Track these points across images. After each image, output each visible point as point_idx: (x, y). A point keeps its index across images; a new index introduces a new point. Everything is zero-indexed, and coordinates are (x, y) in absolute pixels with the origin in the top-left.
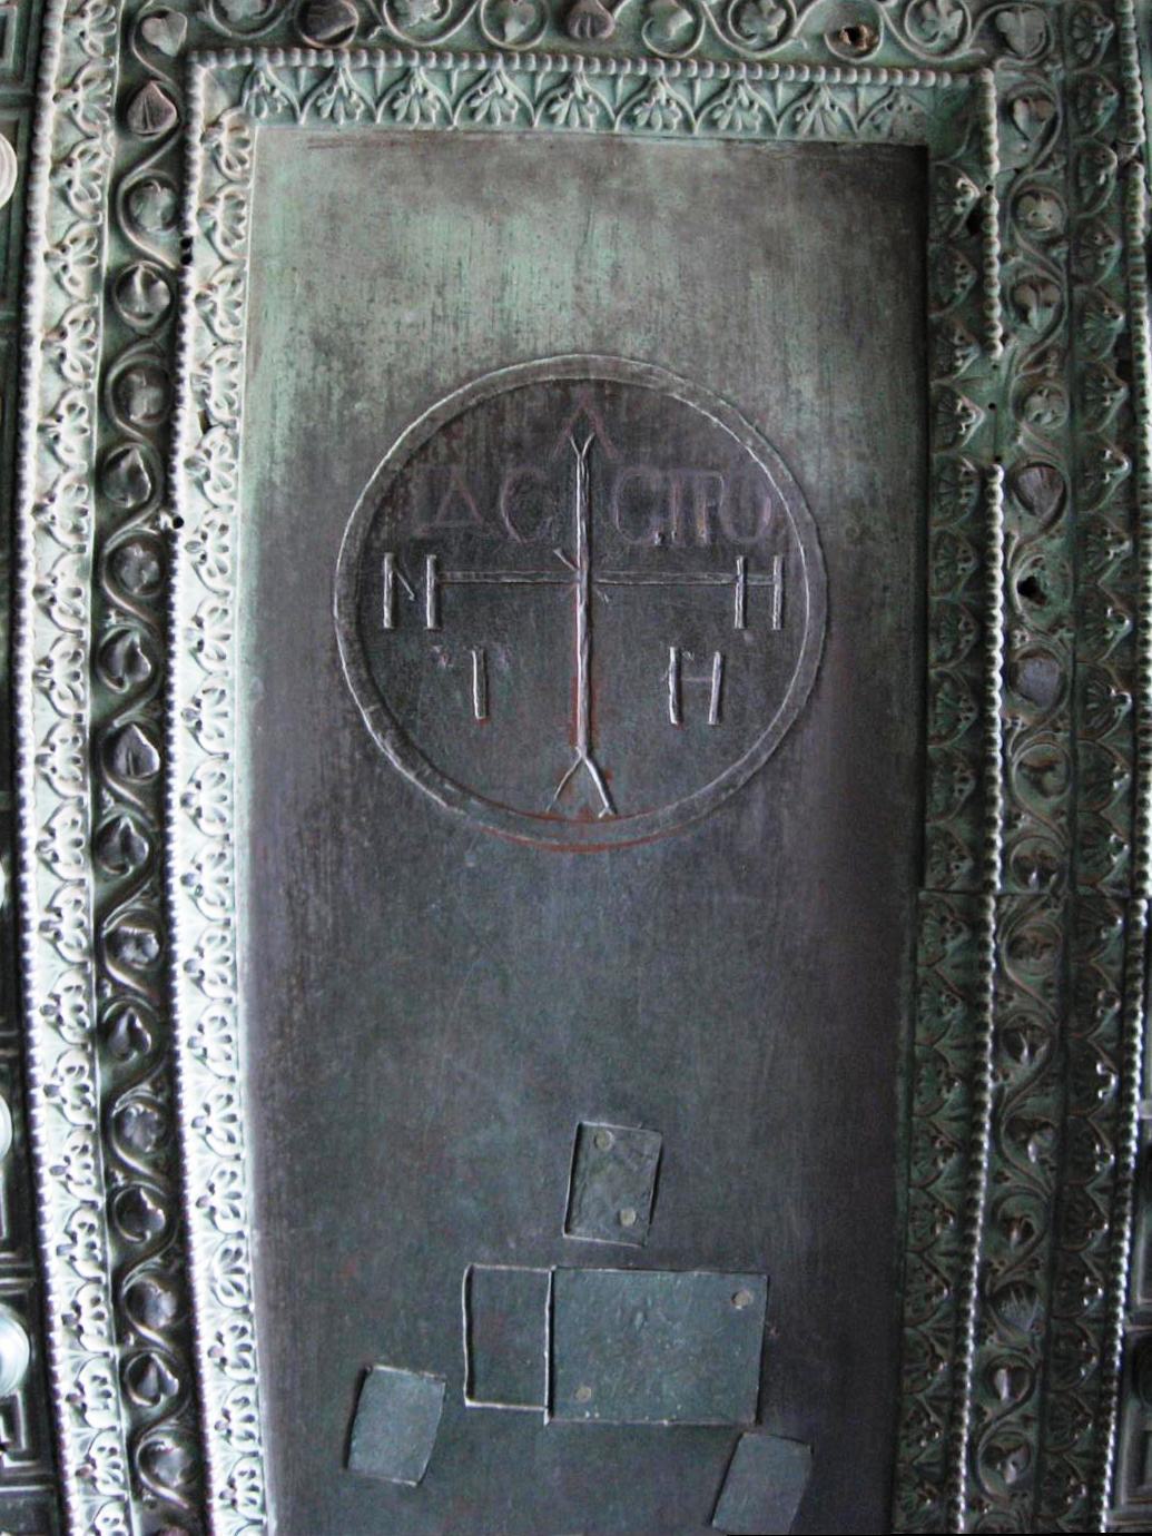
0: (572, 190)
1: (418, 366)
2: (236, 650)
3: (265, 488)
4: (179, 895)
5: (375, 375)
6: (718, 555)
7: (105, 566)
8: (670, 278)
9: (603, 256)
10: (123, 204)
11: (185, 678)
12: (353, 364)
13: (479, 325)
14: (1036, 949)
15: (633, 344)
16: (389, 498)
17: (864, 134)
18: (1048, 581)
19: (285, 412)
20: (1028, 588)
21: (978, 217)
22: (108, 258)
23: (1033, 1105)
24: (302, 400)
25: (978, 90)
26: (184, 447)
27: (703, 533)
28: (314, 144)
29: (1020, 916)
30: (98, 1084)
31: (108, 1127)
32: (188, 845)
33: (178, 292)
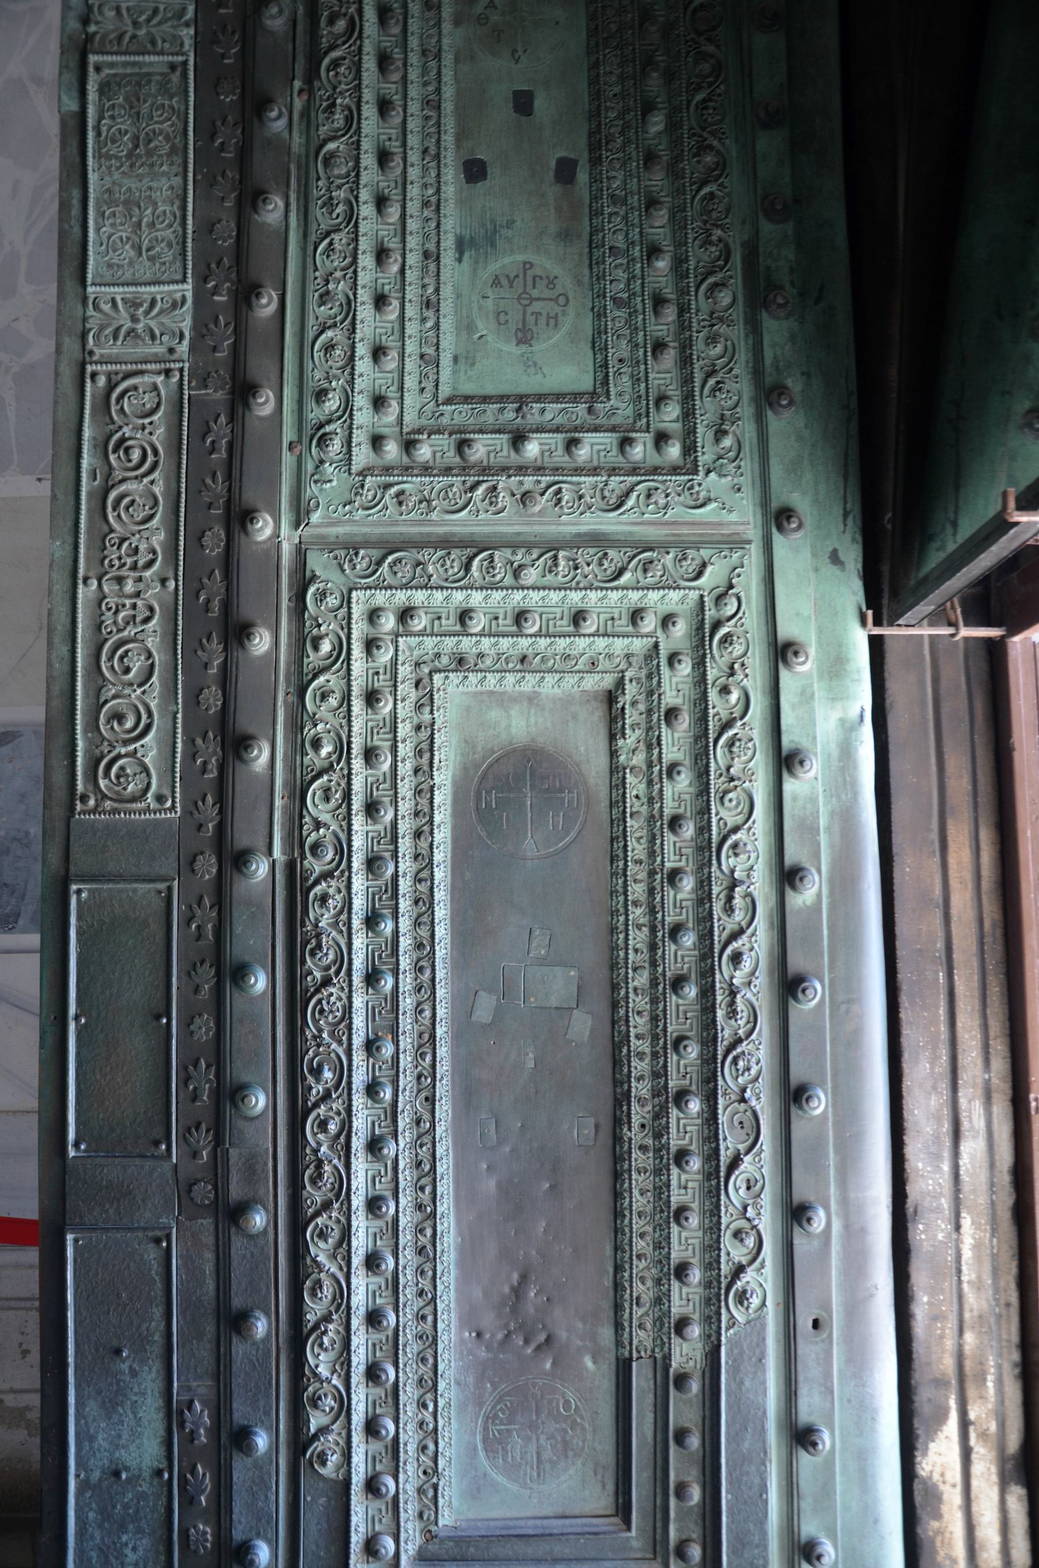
0: (525, 704)
1: (490, 746)
2: (449, 812)
3: (454, 776)
4: (436, 870)
5: (479, 749)
6: (561, 790)
7: (418, 792)
8: (549, 725)
9: (532, 720)
10: (419, 707)
11: (437, 818)
12: (474, 747)
13: (504, 736)
14: (641, 881)
15: (541, 740)
16: (484, 777)
17: (596, 688)
18: (641, 795)
19: (458, 758)
20: (637, 797)
21: (623, 709)
22: (416, 721)
23: (642, 921)
24: (462, 755)
25: (623, 677)
26: (435, 766)
27: (558, 785)
28: (462, 693)
29: (636, 874)
30: (415, 915)
31: (417, 923)
32: (438, 857)
33: (433, 730)
